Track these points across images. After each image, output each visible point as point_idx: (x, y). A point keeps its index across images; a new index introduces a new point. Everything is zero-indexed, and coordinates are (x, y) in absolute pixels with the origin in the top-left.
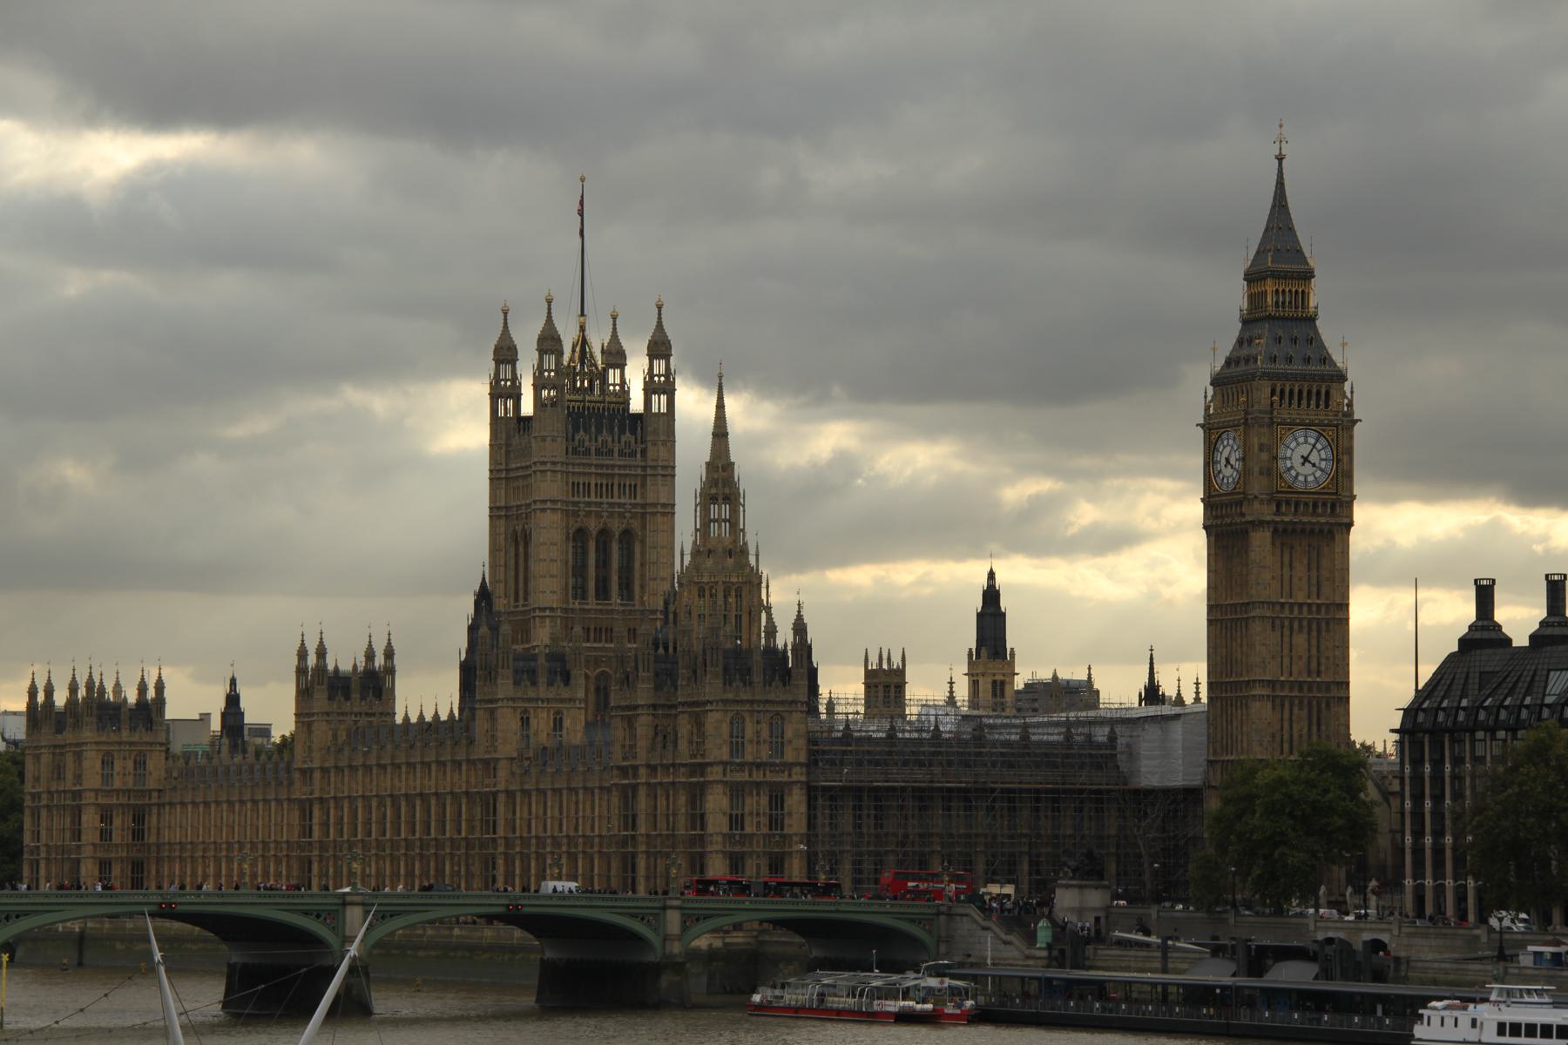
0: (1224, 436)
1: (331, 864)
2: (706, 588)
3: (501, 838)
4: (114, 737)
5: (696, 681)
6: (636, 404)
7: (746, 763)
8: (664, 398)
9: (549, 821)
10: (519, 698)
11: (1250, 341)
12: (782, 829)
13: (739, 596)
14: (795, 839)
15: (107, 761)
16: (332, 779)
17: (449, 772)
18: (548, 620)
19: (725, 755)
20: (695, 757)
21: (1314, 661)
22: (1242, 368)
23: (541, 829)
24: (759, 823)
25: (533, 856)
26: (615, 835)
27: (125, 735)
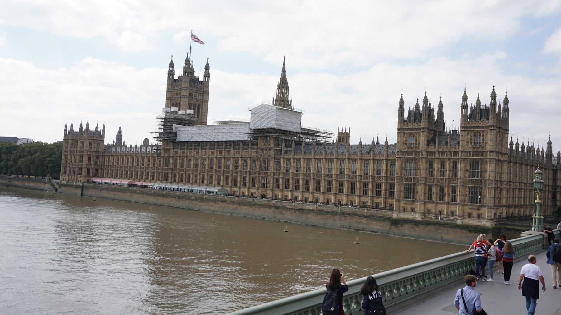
6: (201, 79)
14: (504, 183)
15: (90, 144)
20: (478, 148)
26: (399, 176)
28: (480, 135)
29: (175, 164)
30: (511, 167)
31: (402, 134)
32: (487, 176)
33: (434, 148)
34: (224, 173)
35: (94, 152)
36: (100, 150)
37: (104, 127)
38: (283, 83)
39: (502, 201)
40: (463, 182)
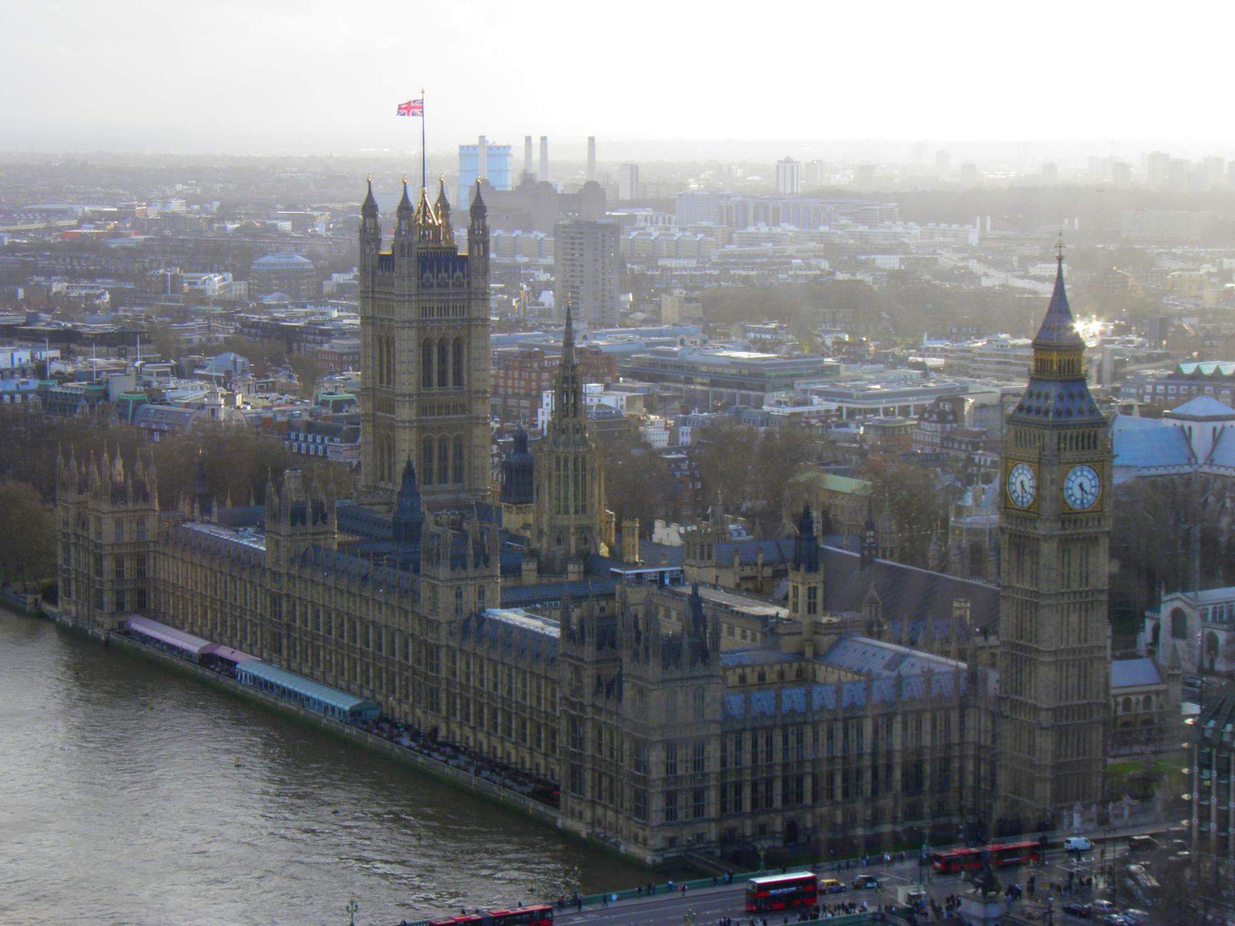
0: (1020, 466)
2: (562, 456)
5: (638, 661)
6: (463, 251)
8: (481, 245)
9: (485, 681)
11: (1039, 396)
12: (703, 769)
13: (584, 462)
14: (713, 776)
15: (119, 524)
16: (297, 586)
18: (407, 404)
21: (1083, 631)
22: (1032, 417)
23: (477, 684)
24: (687, 767)
25: (472, 701)
27: (130, 505)
38: (566, 380)
39: (706, 810)
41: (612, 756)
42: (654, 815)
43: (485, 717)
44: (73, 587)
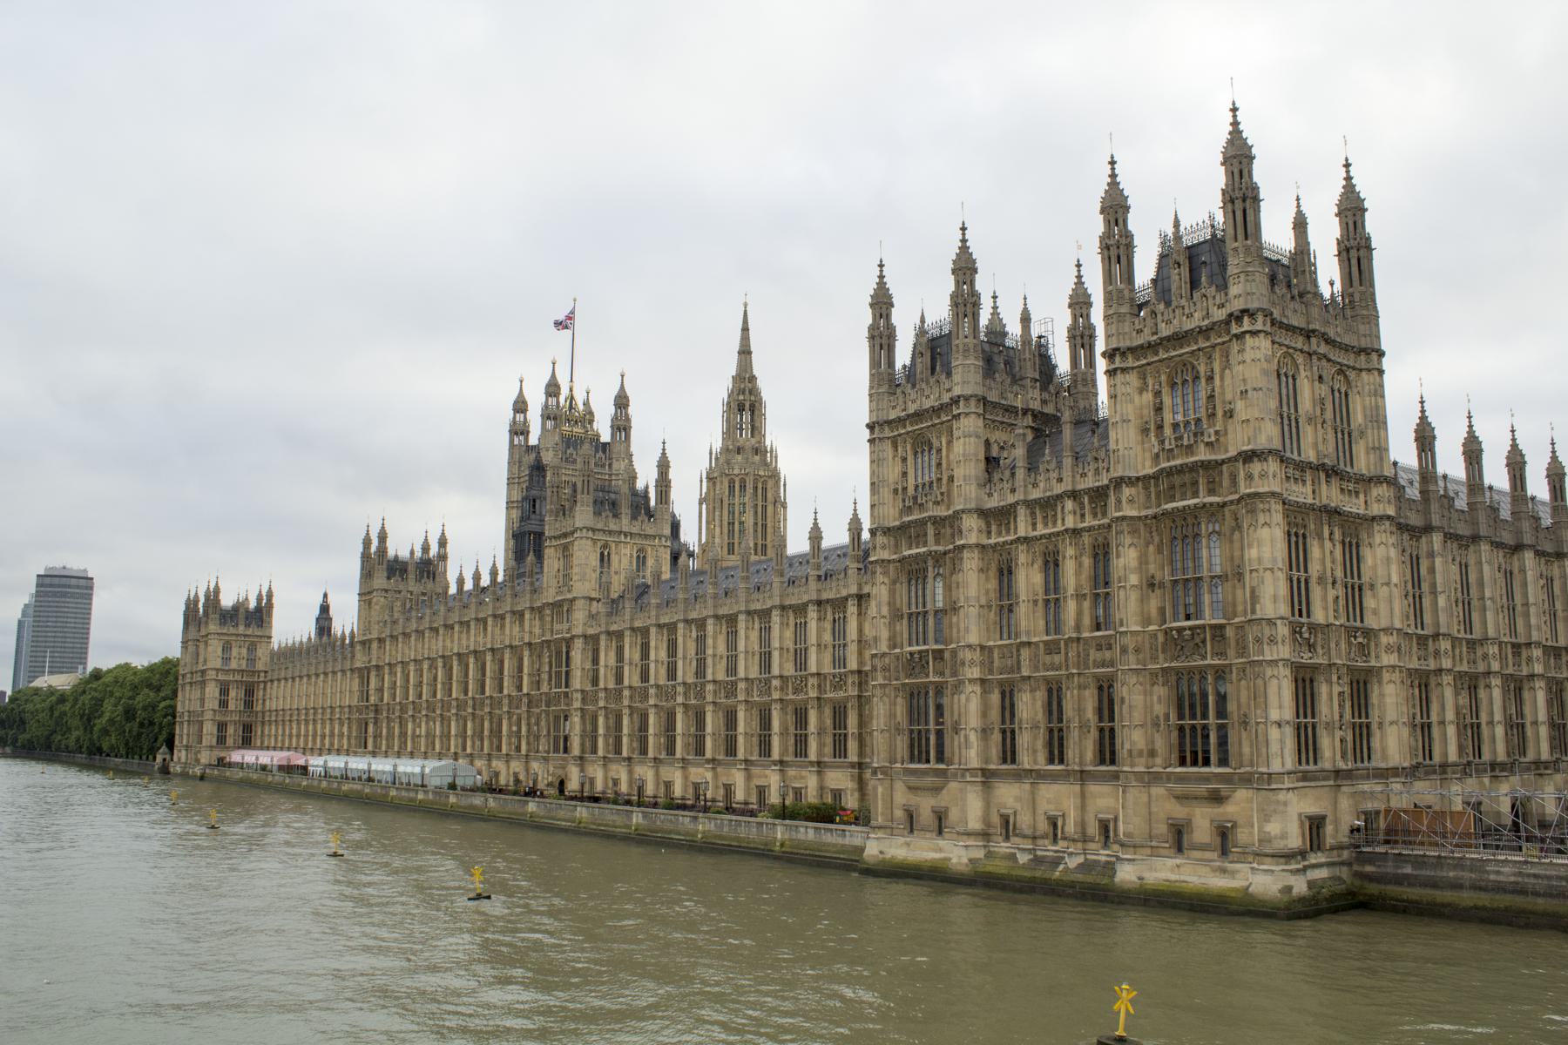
1: (384, 725)
3: (577, 691)
4: (232, 631)
6: (606, 437)
7: (1310, 465)
9: (652, 666)
10: (598, 530)
12: (1362, 621)
13: (765, 490)
15: (227, 648)
16: (388, 648)
17: (508, 625)
19: (1268, 435)
20: (1190, 449)
26: (884, 655)
27: (241, 629)
28: (1196, 378)
29: (380, 690)
30: (1431, 555)
31: (887, 447)
32: (1245, 602)
33: (1013, 491)
34: (474, 709)
35: (239, 671)
36: (260, 666)
37: (270, 595)
39: (1376, 743)
40: (1137, 651)
41: (1054, 624)
42: (1274, 733)
43: (651, 731)
44: (185, 731)
